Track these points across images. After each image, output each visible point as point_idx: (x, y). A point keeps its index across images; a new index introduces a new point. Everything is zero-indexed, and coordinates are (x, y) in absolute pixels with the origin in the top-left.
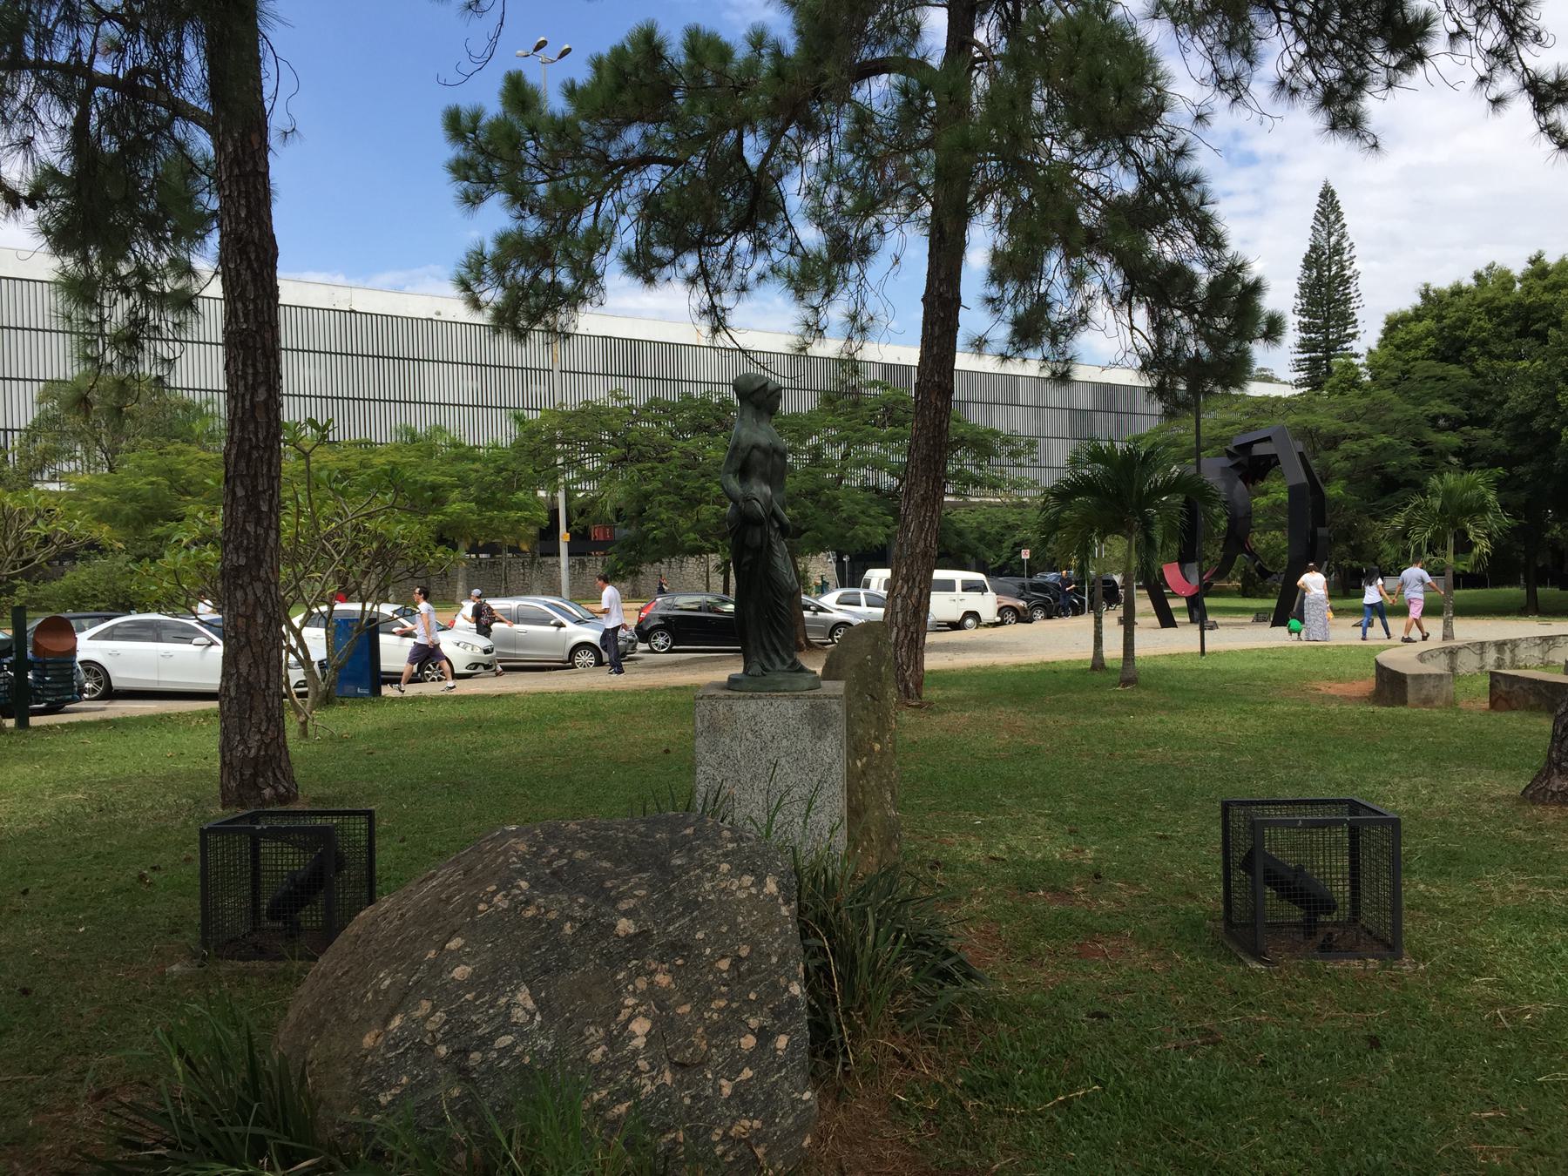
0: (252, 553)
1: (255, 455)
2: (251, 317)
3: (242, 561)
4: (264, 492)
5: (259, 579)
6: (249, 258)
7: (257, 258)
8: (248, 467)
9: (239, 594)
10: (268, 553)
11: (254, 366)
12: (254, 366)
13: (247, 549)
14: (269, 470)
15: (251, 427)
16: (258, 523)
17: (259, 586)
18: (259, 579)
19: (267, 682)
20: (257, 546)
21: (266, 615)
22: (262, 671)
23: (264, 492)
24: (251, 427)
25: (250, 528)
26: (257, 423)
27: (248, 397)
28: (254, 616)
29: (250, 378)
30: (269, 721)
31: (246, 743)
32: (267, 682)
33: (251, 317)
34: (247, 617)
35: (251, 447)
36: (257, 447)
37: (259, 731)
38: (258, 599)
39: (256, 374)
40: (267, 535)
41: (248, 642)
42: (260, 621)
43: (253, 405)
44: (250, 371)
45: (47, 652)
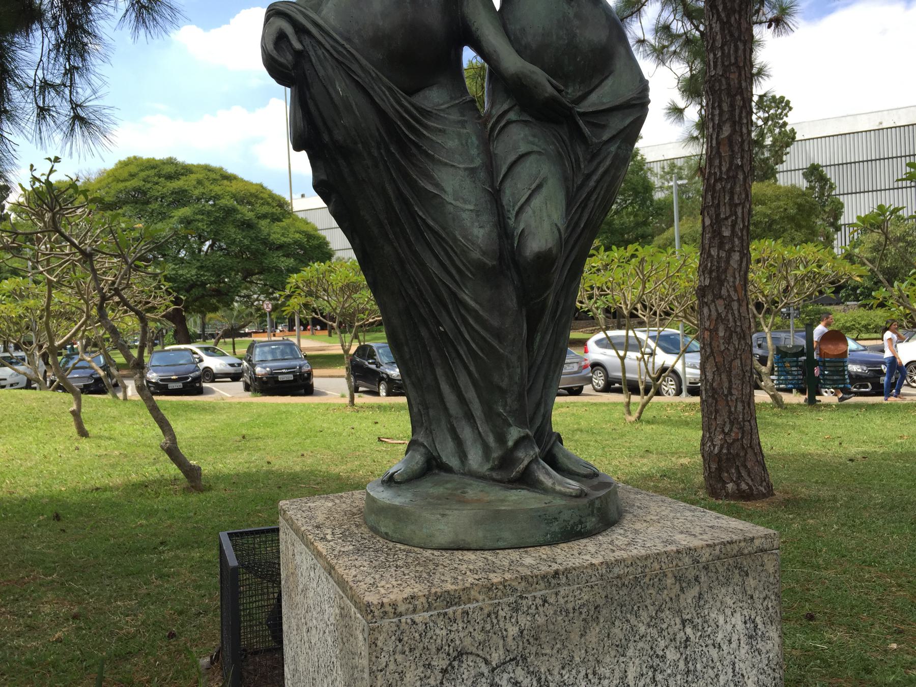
0: (714, 274)
1: (719, 186)
2: (719, 63)
3: (707, 283)
4: (726, 218)
5: (721, 297)
6: (718, 10)
7: (725, 8)
8: (713, 198)
9: (706, 310)
10: (730, 271)
11: (720, 106)
12: (720, 106)
13: (711, 272)
14: (731, 198)
15: (717, 162)
16: (721, 246)
17: (720, 304)
18: (721, 297)
19: (730, 388)
20: (718, 268)
21: (727, 329)
22: (724, 376)
23: (726, 218)
24: (717, 162)
25: (714, 252)
26: (720, 157)
27: (714, 137)
28: (716, 330)
29: (717, 118)
30: (732, 423)
31: (712, 441)
32: (730, 388)
33: (719, 63)
34: (710, 331)
35: (716, 181)
36: (721, 179)
37: (723, 431)
38: (719, 314)
39: (720, 115)
40: (729, 257)
41: (712, 352)
42: (721, 334)
43: (718, 143)
44: (717, 112)
45: (827, 355)
